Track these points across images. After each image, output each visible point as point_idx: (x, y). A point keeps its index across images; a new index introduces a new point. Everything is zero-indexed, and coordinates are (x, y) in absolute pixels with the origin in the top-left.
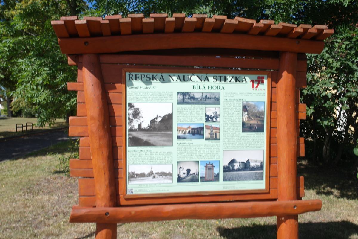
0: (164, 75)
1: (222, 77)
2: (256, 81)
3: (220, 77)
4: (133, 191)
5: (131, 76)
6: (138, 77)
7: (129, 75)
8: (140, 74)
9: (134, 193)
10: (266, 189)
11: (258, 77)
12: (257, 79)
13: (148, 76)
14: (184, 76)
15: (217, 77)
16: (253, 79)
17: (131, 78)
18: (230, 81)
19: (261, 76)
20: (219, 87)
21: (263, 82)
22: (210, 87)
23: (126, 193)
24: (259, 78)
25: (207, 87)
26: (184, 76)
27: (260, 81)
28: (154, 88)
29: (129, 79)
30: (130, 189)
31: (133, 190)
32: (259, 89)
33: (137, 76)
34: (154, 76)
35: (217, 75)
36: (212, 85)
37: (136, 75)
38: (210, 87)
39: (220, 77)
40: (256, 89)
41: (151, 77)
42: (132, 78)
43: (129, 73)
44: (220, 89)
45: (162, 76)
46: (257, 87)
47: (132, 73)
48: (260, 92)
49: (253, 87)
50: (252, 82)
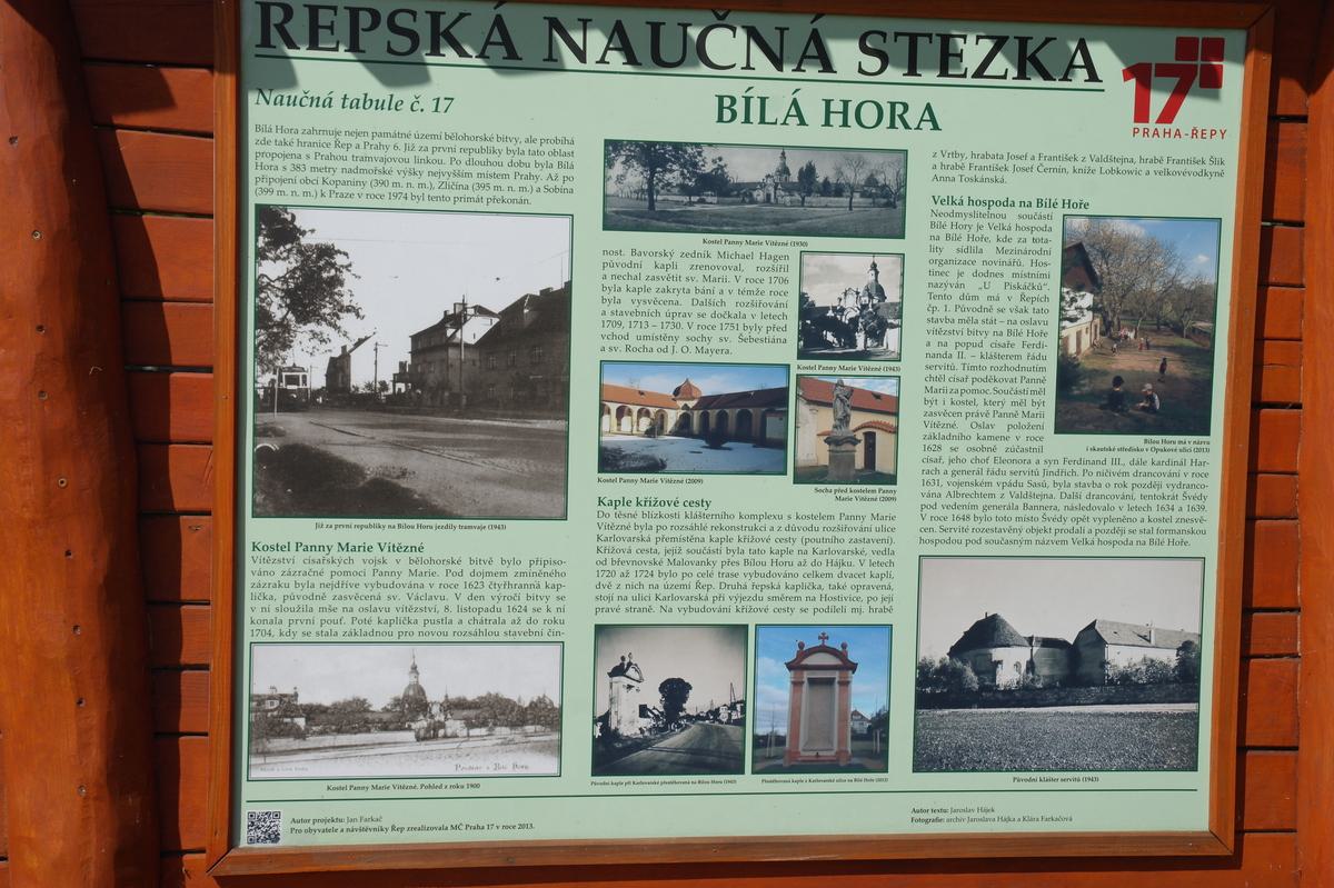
1: (922, 42)
2: (1164, 70)
3: (913, 38)
4: (283, 826)
9: (288, 841)
10: (1214, 836)
11: (1180, 41)
12: (1169, 58)
14: (655, 28)
15: (890, 37)
16: (1143, 60)
17: (281, 28)
18: (979, 74)
19: (1200, 34)
20: (899, 109)
21: (1212, 81)
22: (837, 106)
23: (232, 840)
24: (1185, 48)
25: (814, 113)
26: (655, 28)
28: (443, 104)
29: (266, 42)
30: (259, 809)
31: (277, 815)
32: (1186, 130)
34: (444, 23)
35: (890, 25)
36: (856, 94)
38: (837, 106)
39: (914, 39)
40: (1161, 127)
42: (287, 26)
44: (907, 126)
45: (499, 22)
46: (1168, 115)
48: (1185, 148)
49: (1141, 114)
50: (1133, 82)
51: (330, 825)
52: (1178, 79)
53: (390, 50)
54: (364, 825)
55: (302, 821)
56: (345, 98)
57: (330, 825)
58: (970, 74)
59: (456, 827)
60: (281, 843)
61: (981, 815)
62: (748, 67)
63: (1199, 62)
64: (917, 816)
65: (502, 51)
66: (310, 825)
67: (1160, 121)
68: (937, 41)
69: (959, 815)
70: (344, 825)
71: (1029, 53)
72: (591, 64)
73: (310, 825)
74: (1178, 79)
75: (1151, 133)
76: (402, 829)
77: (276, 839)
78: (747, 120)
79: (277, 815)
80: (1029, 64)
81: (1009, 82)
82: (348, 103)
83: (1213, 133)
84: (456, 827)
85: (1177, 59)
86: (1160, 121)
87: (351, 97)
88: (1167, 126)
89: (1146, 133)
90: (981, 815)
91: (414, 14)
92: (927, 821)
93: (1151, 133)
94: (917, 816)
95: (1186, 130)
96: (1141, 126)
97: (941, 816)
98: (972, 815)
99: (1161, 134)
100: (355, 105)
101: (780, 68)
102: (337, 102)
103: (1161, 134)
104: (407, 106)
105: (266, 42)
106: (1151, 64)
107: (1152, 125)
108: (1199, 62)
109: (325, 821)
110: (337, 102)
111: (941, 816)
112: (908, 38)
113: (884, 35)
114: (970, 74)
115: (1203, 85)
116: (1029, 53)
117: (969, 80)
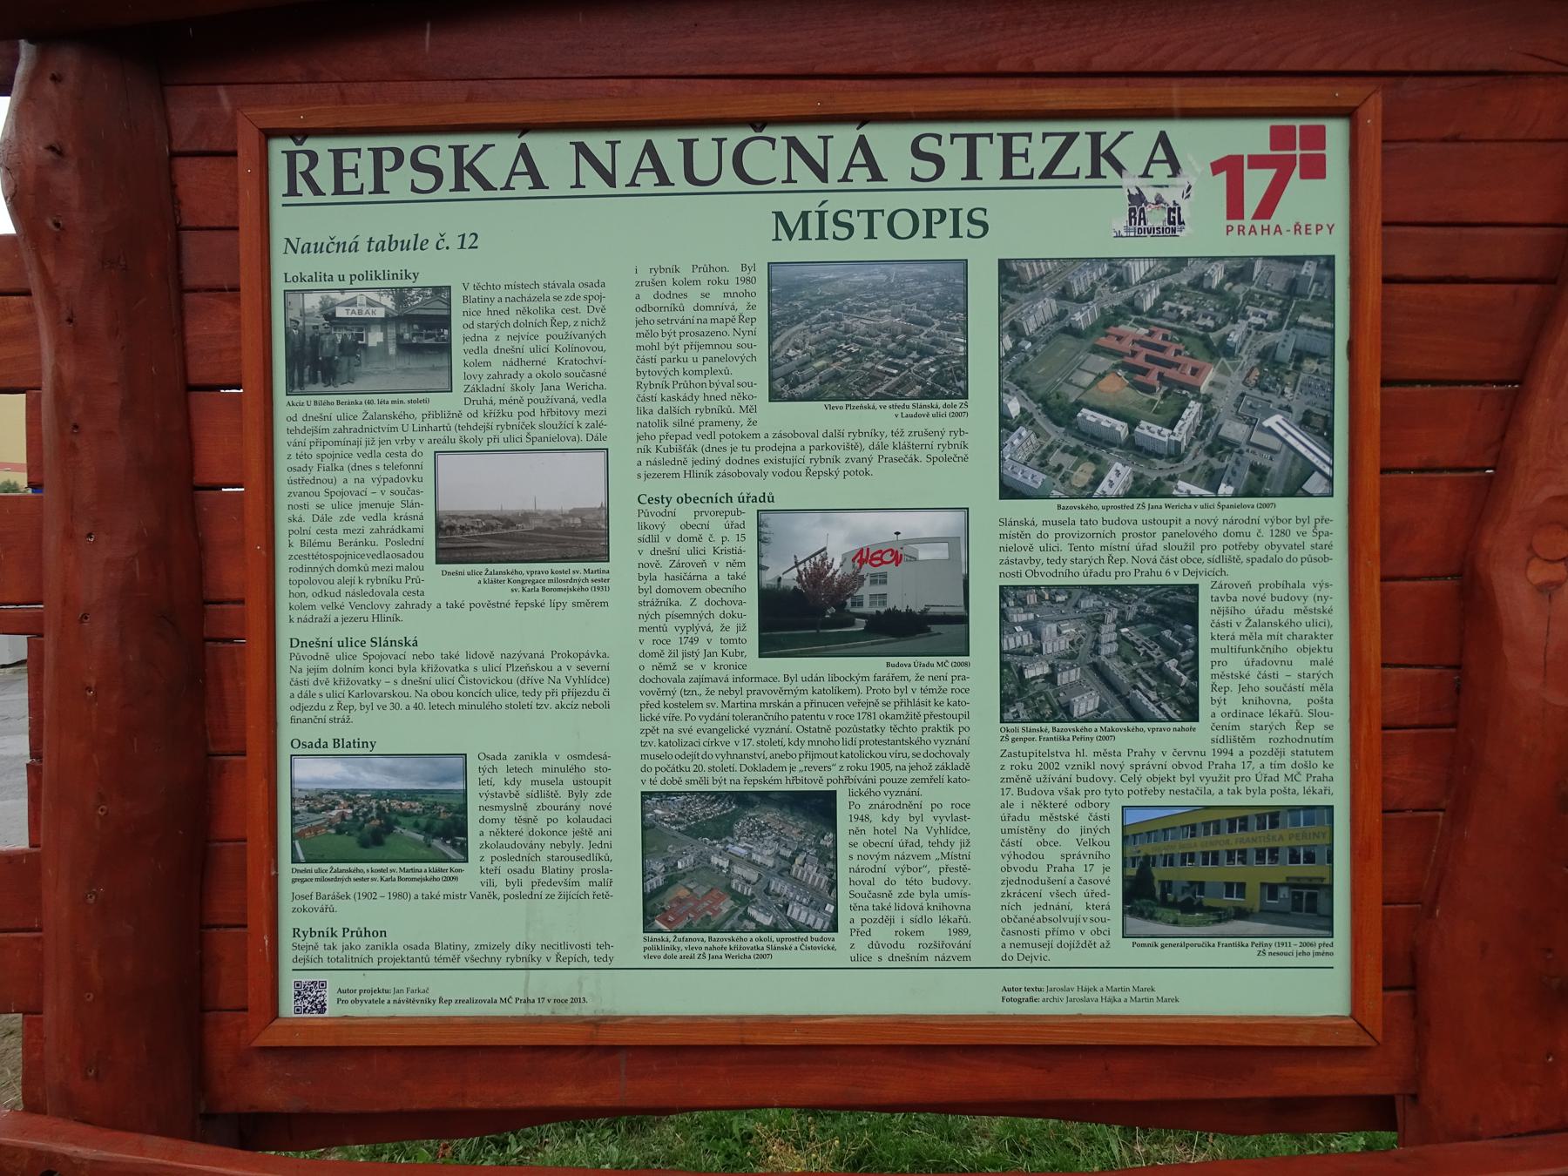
0: (538, 144)
2: (1258, 162)
3: (972, 140)
4: (330, 997)
5: (302, 162)
6: (355, 171)
7: (291, 156)
8: (365, 143)
13: (426, 157)
14: (688, 145)
15: (946, 139)
18: (1048, 173)
19: (1298, 123)
24: (1280, 138)
26: (688, 145)
27: (1292, 161)
28: (469, 241)
29: (292, 191)
30: (306, 978)
31: (323, 984)
32: (1286, 225)
33: (349, 161)
35: (946, 130)
37: (338, 155)
39: (972, 140)
40: (1258, 223)
41: (446, 163)
43: (289, 145)
46: (1266, 209)
47: (310, 144)
49: (1235, 209)
50: (1223, 175)
51: (376, 996)
52: (1274, 171)
53: (414, 189)
54: (411, 996)
55: (348, 991)
56: (371, 241)
57: (376, 996)
58: (1037, 174)
59: (505, 1001)
60: (326, 1014)
61: (1081, 995)
62: (789, 180)
63: (1298, 152)
64: (1008, 995)
65: (528, 180)
66: (356, 995)
67: (1257, 216)
68: (999, 141)
69: (1056, 994)
70: (391, 997)
71: (1103, 149)
72: (621, 188)
73: (356, 995)
74: (1274, 171)
75: (1247, 231)
76: (450, 1002)
77: (322, 1010)
78: (805, 237)
79: (323, 984)
80: (1103, 162)
81: (1081, 181)
82: (373, 246)
83: (1319, 228)
84: (505, 1001)
85: (1272, 148)
86: (1257, 216)
87: (376, 240)
88: (1265, 223)
89: (1241, 230)
90: (1081, 995)
91: (437, 149)
92: (1020, 1001)
93: (1247, 231)
94: (1008, 995)
95: (1286, 225)
96: (1236, 223)
97: (1035, 995)
98: (1071, 995)
99: (1259, 230)
100: (381, 247)
101: (612, 184)
102: (363, 246)
103: (1259, 230)
104: (432, 244)
105: (292, 191)
106: (1242, 157)
107: (1248, 221)
108: (1298, 152)
109: (372, 991)
110: (363, 246)
111: (1035, 995)
112: (965, 140)
113: (939, 137)
114: (1036, 175)
115: (1303, 176)
116: (1103, 149)
117: (1036, 182)
